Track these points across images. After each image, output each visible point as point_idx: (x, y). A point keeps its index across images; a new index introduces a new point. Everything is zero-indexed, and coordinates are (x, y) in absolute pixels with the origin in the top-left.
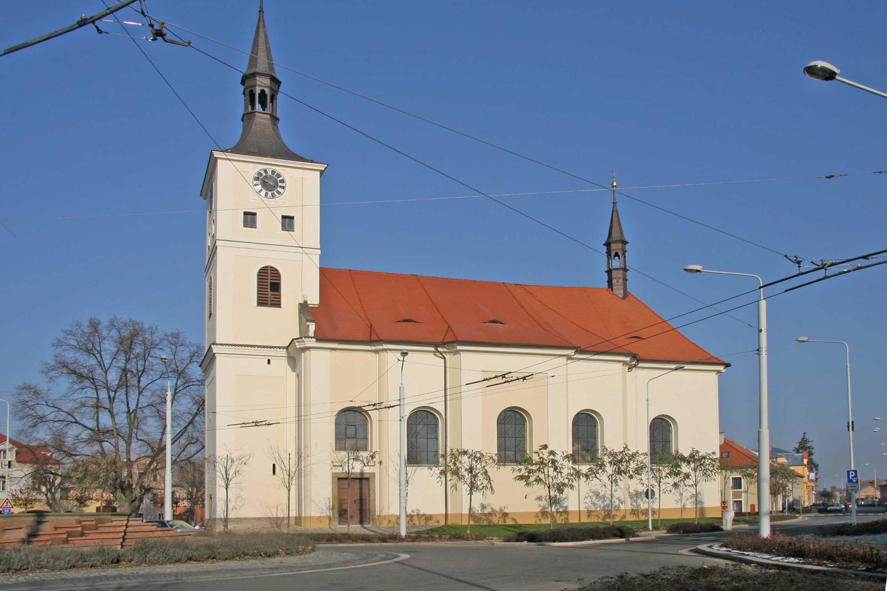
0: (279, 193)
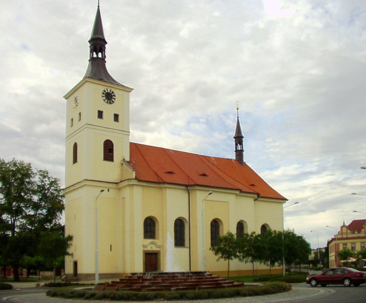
0: (113, 102)
